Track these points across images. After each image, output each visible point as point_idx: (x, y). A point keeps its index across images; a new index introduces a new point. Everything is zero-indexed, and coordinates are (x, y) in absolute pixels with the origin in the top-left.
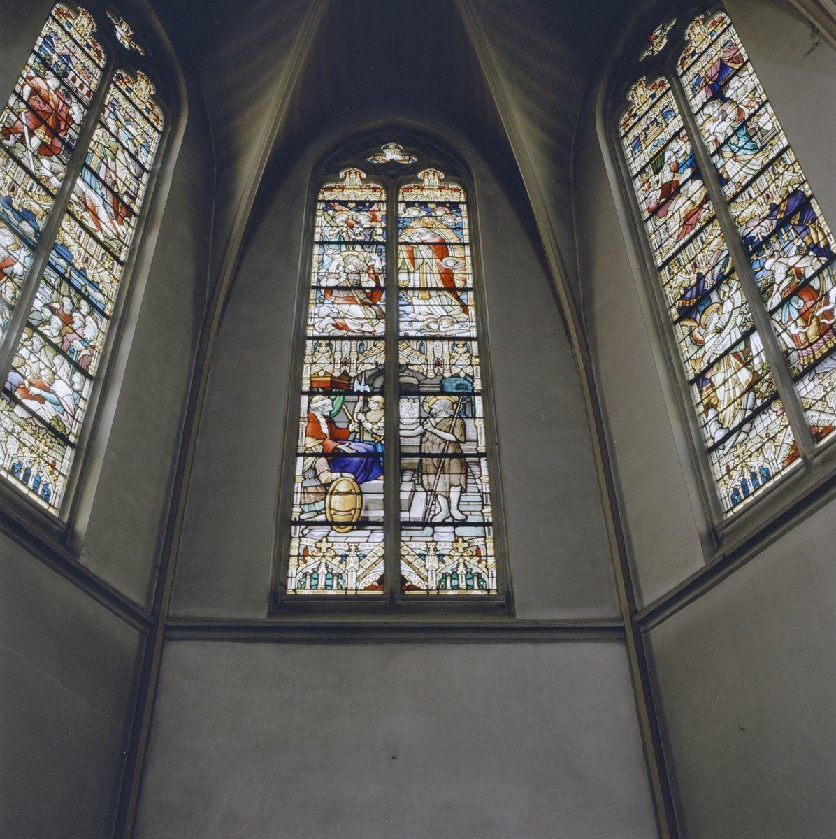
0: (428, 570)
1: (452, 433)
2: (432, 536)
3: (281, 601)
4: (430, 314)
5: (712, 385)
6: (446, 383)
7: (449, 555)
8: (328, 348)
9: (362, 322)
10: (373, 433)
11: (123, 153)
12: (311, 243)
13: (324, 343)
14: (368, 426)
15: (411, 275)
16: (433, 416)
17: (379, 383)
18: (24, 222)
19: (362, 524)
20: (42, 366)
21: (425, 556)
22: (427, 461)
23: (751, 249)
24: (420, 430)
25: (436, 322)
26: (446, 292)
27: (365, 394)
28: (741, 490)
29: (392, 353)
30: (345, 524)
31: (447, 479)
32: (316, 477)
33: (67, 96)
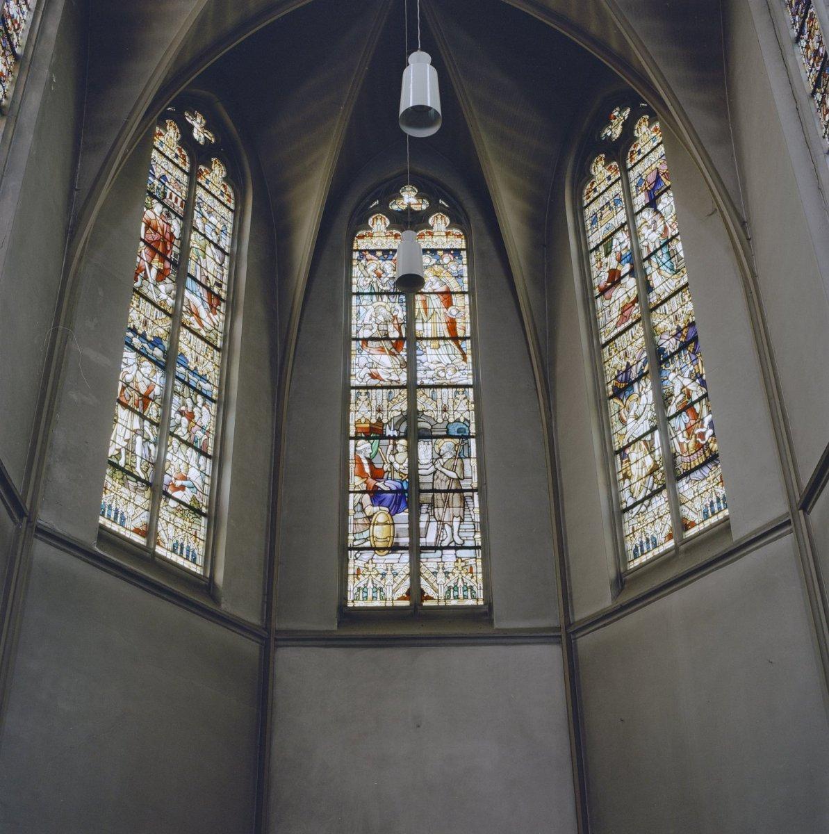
0: (438, 584)
1: (455, 472)
2: (441, 557)
4: (439, 363)
5: (629, 461)
6: (451, 428)
7: (452, 573)
8: (367, 396)
9: (390, 371)
10: (400, 473)
11: (210, 246)
13: (363, 391)
14: (397, 466)
15: (425, 324)
16: (441, 457)
17: (403, 427)
18: (156, 349)
19: (395, 548)
20: (180, 462)
21: (436, 573)
22: (438, 496)
23: (662, 359)
24: (432, 469)
25: (443, 370)
26: (450, 342)
27: (394, 438)
28: (639, 548)
29: (412, 400)
30: (384, 549)
31: (451, 512)
32: (363, 510)
33: (169, 216)
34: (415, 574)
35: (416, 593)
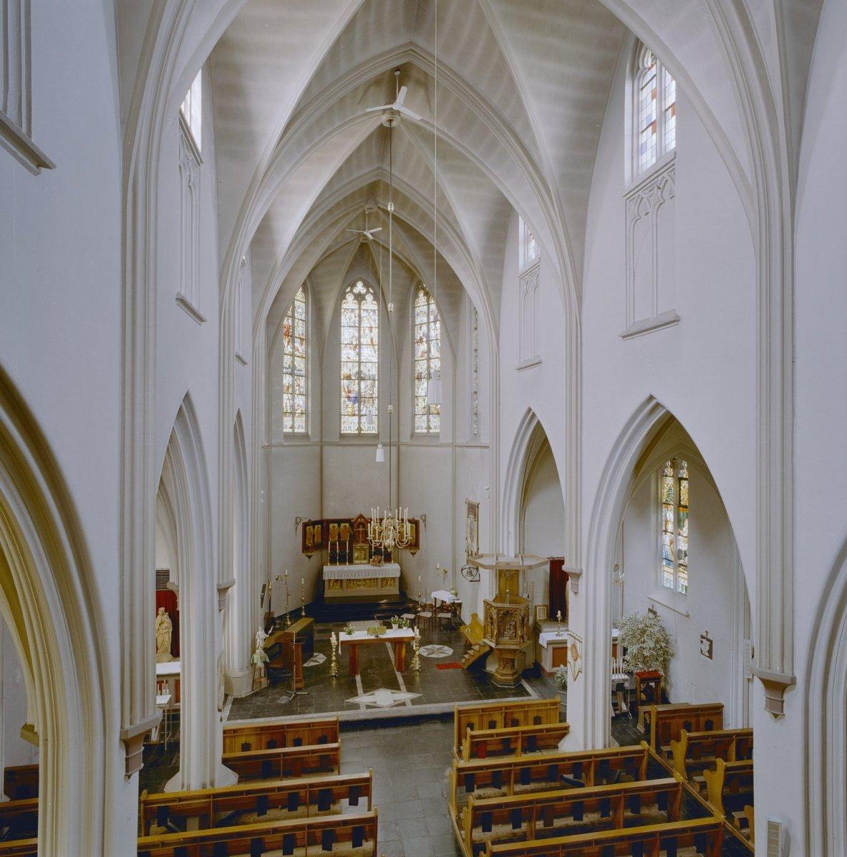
3: (343, 436)
12: (341, 327)
19: (354, 415)
22: (366, 399)
34: (359, 423)
35: (360, 429)
